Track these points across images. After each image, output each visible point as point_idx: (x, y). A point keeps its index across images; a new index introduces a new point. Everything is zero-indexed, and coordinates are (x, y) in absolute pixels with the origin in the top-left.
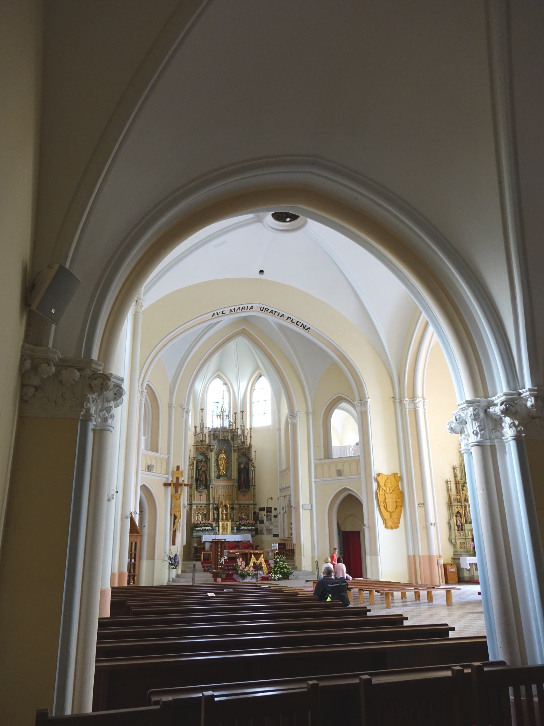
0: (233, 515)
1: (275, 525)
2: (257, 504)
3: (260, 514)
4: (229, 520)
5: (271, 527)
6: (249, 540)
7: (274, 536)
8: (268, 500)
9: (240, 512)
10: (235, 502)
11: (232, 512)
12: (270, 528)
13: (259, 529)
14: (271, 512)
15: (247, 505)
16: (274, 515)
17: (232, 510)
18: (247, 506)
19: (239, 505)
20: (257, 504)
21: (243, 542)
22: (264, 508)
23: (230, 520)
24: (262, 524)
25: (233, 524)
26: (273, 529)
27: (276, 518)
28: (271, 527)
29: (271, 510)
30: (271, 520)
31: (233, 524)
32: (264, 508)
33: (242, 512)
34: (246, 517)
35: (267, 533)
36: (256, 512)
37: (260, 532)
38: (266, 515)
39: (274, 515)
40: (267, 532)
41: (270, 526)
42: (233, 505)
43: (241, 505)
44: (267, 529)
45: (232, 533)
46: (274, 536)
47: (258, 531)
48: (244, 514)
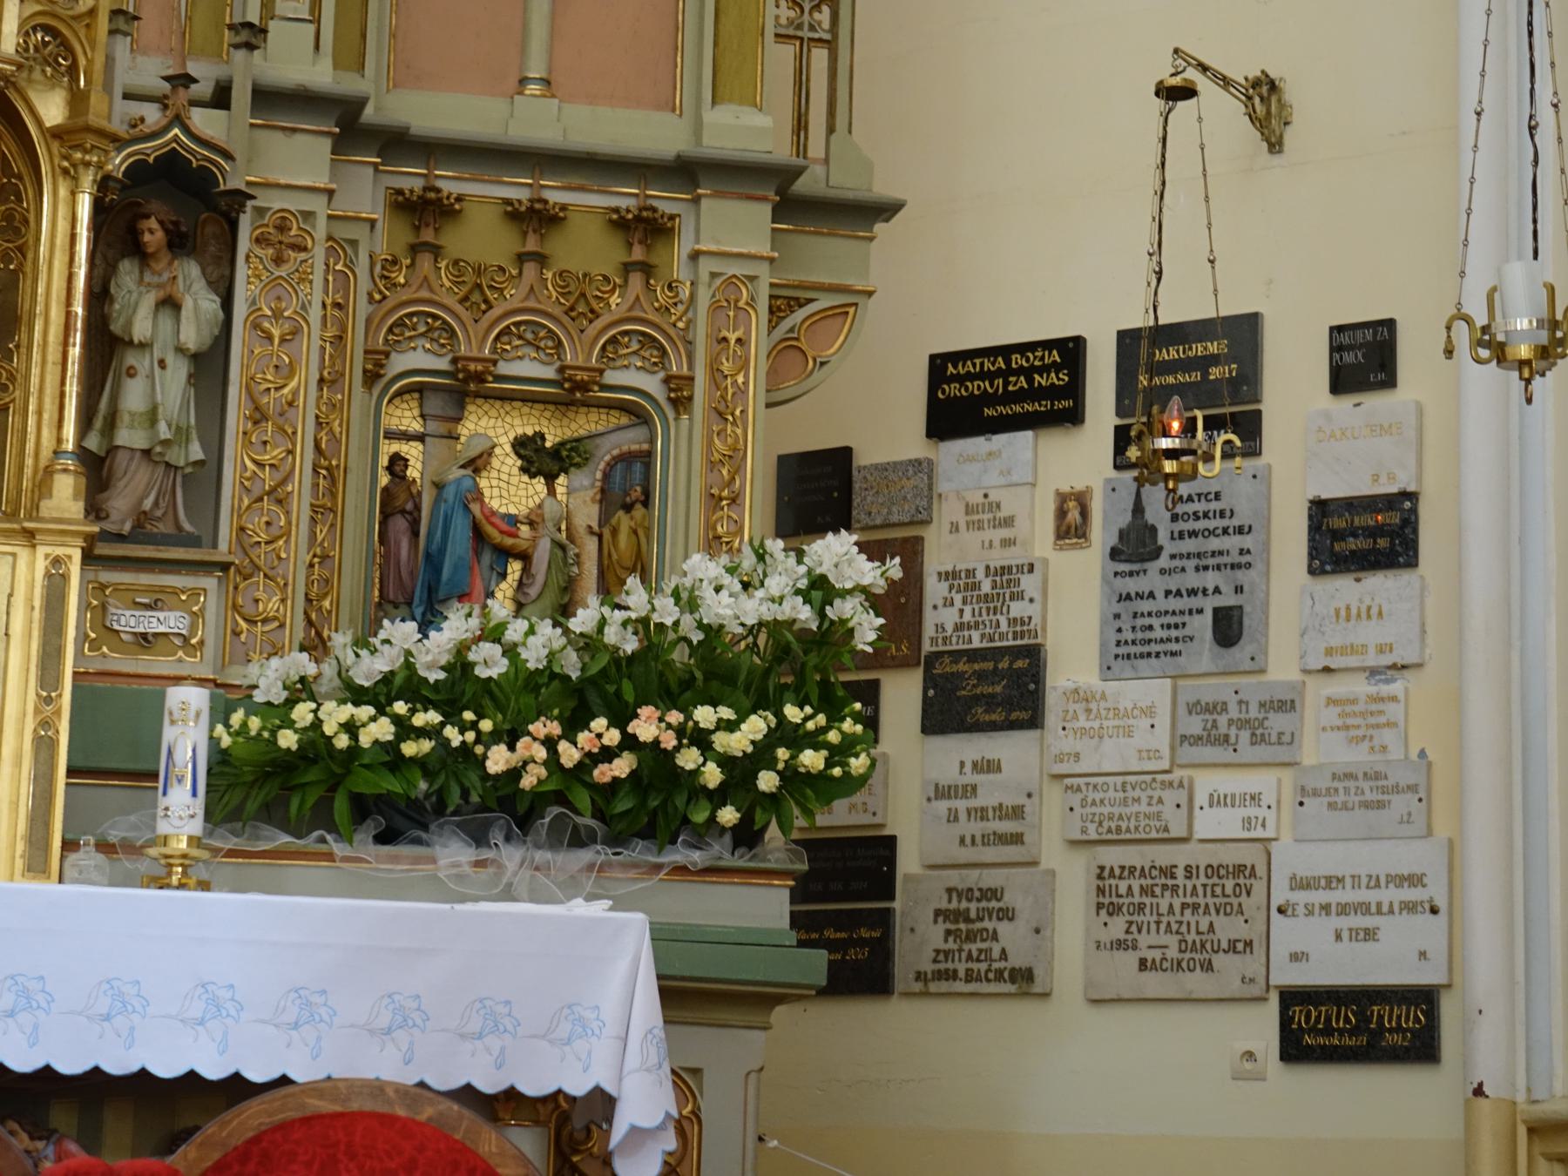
0: (174, 384)
1: (1355, 757)
2: (886, 210)
3: (949, 511)
4: (46, 476)
5: (1216, 801)
6: (578, 1087)
7: (1294, 1049)
8: (1176, 93)
9: (418, 358)
10: (252, 36)
11: (170, 304)
12: (1210, 823)
13: (908, 862)
14: (1249, 428)
15: (624, 198)
16: (1320, 509)
17: (179, 243)
18: (621, 224)
19: (410, 177)
20: (886, 210)
21: (250, 1118)
22: (1072, 351)
23: (66, 496)
24: (1009, 748)
25: (170, 621)
26: (1290, 859)
27: (1380, 585)
28: (1216, 801)
29: (1248, 381)
30: (1228, 628)
31: (170, 621)
32: (1072, 351)
33: (474, 344)
34: (587, 514)
35: (1122, 969)
36: (865, 457)
37: (934, 935)
38: (1102, 534)
39: (1320, 509)
40: (1117, 926)
41: (1207, 783)
42: (205, 121)
43: (451, 182)
44: (1113, 857)
45: (87, 857)
46: (1294, 1049)
47: (884, 919)
48: (523, 423)
